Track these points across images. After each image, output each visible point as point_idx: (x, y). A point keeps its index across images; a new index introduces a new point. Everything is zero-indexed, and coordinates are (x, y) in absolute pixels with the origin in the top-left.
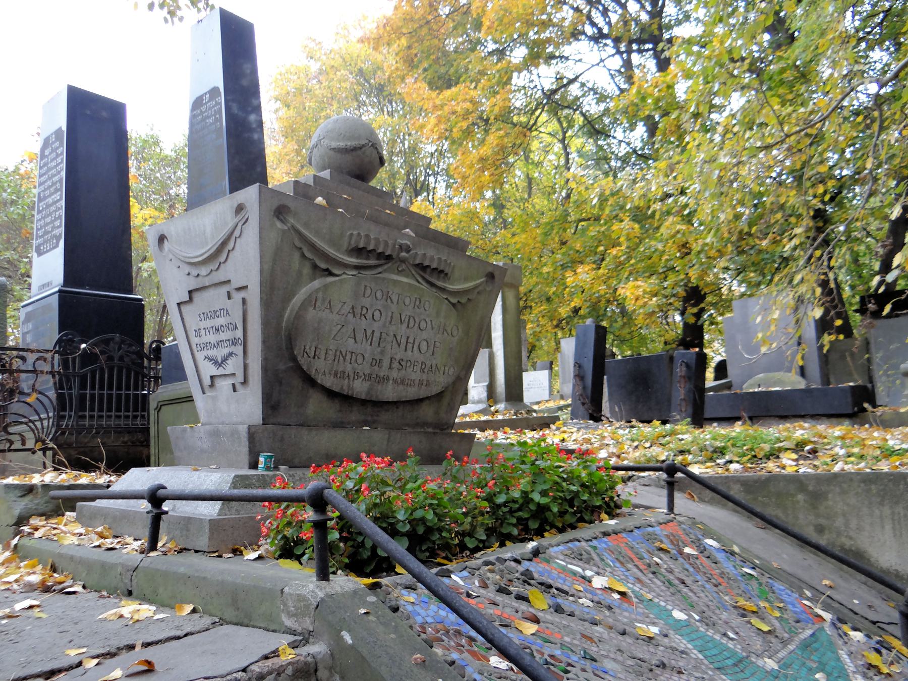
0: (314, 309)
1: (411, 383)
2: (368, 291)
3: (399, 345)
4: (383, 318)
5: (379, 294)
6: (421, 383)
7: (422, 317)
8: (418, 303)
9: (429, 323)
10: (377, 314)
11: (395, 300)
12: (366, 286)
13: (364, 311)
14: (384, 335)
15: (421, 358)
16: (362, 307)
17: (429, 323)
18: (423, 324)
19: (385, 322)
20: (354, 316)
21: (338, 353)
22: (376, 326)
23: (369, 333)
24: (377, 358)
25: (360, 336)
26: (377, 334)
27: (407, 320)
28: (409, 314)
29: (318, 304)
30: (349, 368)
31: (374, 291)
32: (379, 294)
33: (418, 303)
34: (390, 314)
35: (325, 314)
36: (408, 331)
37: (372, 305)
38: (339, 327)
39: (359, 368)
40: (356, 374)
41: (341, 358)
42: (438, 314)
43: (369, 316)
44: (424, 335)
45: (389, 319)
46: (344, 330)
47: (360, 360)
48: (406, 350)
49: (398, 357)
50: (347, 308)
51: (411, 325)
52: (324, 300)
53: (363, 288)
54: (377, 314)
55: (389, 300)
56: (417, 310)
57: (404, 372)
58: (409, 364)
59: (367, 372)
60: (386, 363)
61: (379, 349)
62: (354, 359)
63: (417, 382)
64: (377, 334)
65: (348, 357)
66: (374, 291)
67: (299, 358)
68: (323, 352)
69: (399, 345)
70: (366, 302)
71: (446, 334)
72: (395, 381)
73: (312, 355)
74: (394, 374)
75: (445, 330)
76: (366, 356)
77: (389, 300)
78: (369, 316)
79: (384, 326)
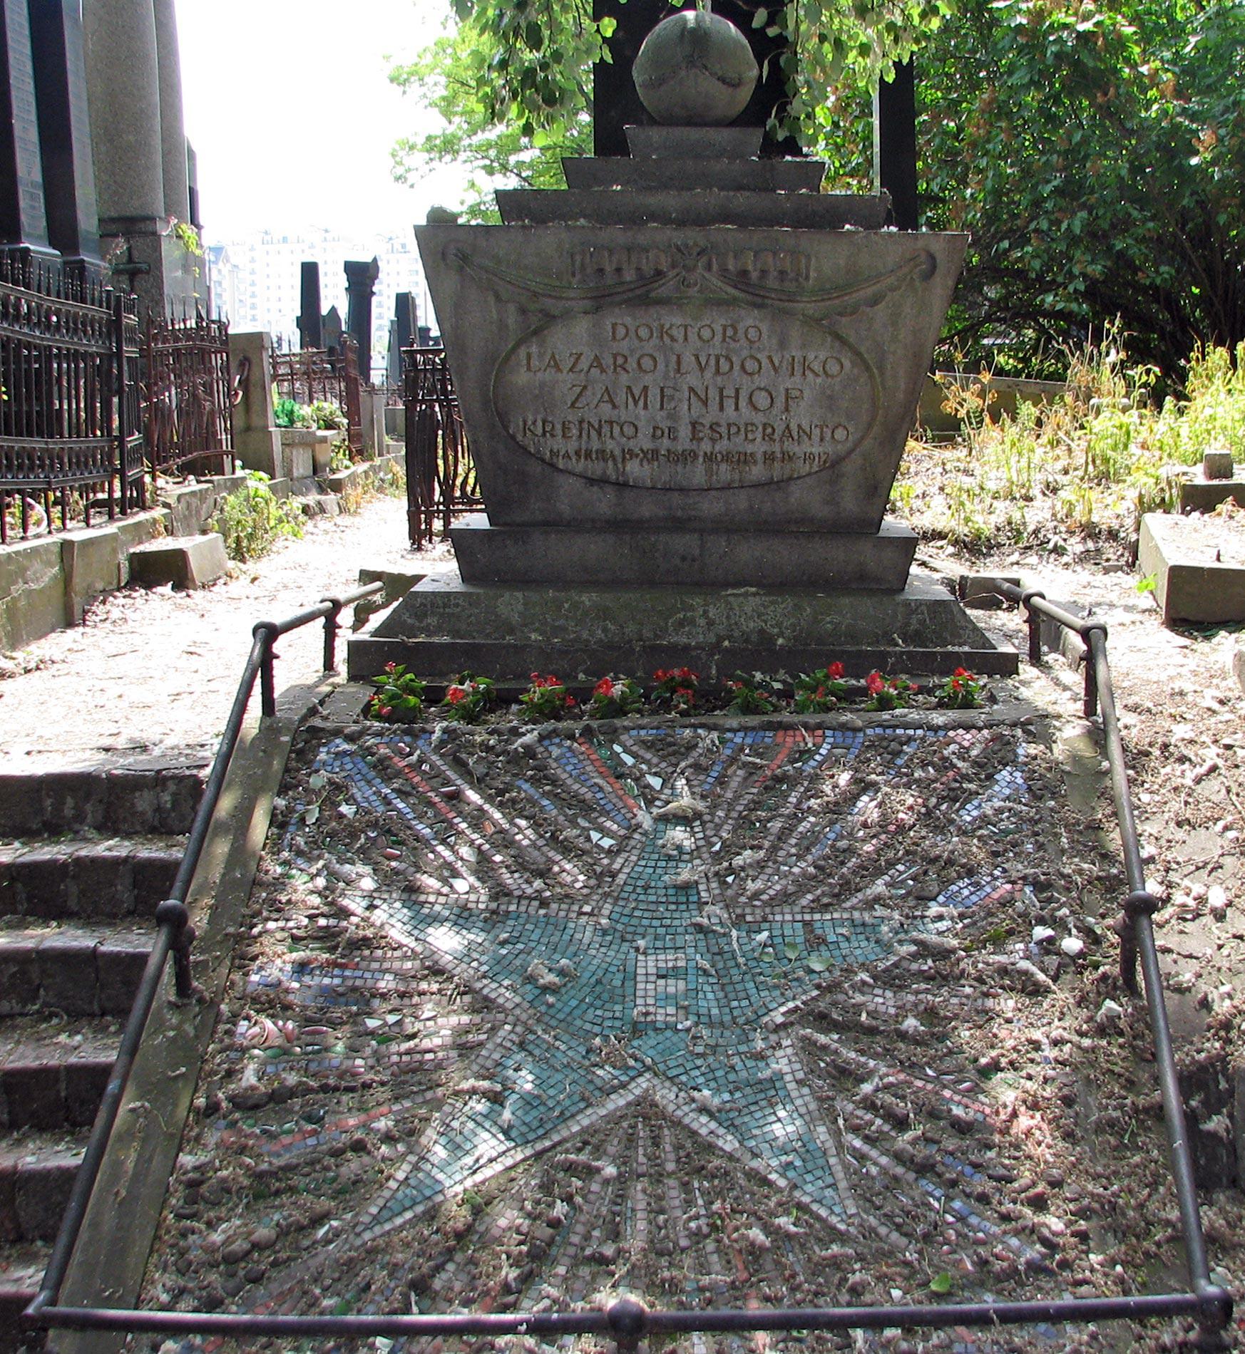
0: (529, 369)
1: (745, 459)
2: (621, 331)
3: (705, 403)
4: (661, 367)
5: (643, 332)
6: (769, 458)
7: (745, 353)
8: (730, 332)
9: (765, 362)
10: (647, 363)
11: (681, 338)
12: (614, 326)
13: (620, 361)
14: (668, 392)
15: (759, 419)
16: (615, 357)
17: (765, 362)
18: (751, 366)
19: (667, 372)
20: (603, 371)
21: (585, 426)
22: (648, 379)
23: (637, 392)
24: (665, 425)
25: (621, 397)
26: (654, 395)
27: (712, 362)
28: (717, 352)
29: (535, 362)
30: (610, 445)
31: (632, 329)
32: (643, 332)
33: (730, 332)
34: (674, 358)
35: (549, 375)
36: (719, 379)
37: (632, 351)
38: (578, 390)
39: (632, 443)
40: (629, 454)
41: (593, 433)
42: (783, 344)
43: (632, 364)
44: (760, 381)
45: (673, 365)
46: (588, 393)
47: (629, 430)
48: (722, 408)
49: (707, 421)
50: (584, 364)
51: (724, 366)
52: (541, 356)
53: (609, 328)
54: (647, 363)
55: (666, 337)
56: (733, 345)
57: (725, 442)
58: (734, 430)
59: (647, 445)
60: (684, 432)
61: (663, 413)
62: (616, 430)
63: (759, 457)
64: (654, 395)
65: (606, 429)
66: (632, 329)
67: (519, 438)
68: (559, 427)
69: (705, 403)
70: (624, 346)
71: (809, 375)
72: (709, 458)
73: (539, 431)
74: (706, 446)
75: (806, 368)
76: (640, 425)
77: (666, 337)
78: (632, 364)
79: (666, 377)
